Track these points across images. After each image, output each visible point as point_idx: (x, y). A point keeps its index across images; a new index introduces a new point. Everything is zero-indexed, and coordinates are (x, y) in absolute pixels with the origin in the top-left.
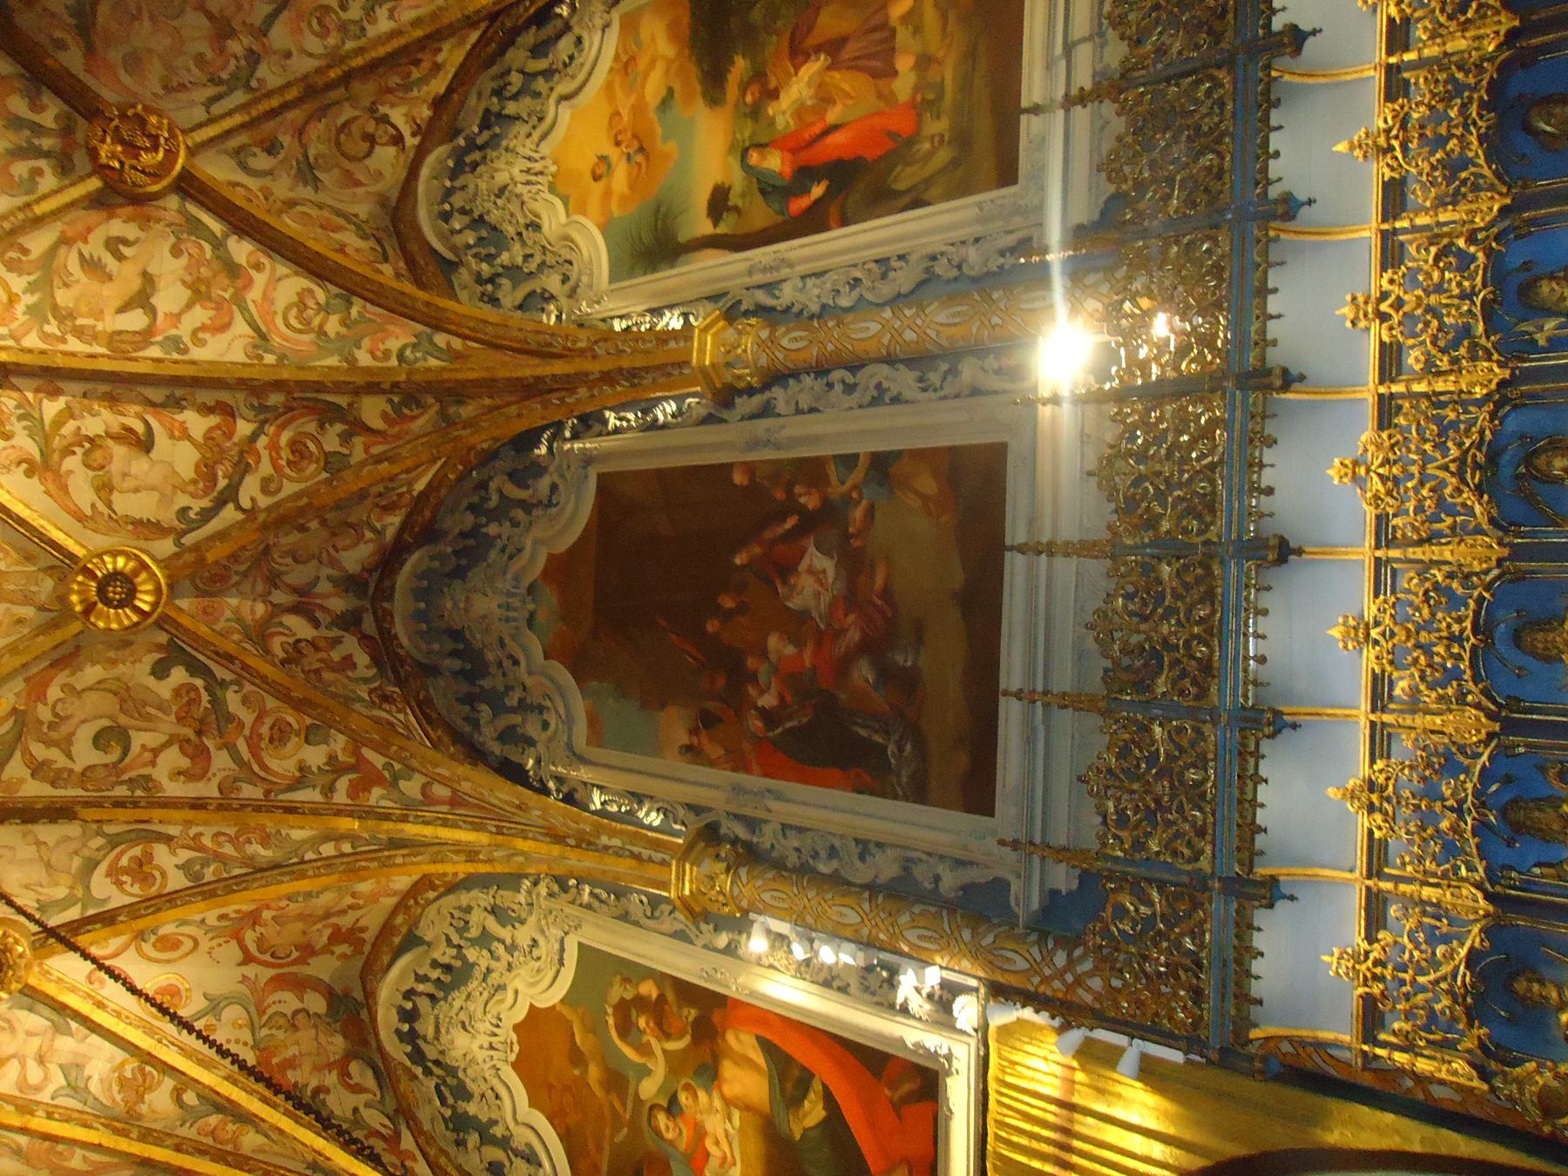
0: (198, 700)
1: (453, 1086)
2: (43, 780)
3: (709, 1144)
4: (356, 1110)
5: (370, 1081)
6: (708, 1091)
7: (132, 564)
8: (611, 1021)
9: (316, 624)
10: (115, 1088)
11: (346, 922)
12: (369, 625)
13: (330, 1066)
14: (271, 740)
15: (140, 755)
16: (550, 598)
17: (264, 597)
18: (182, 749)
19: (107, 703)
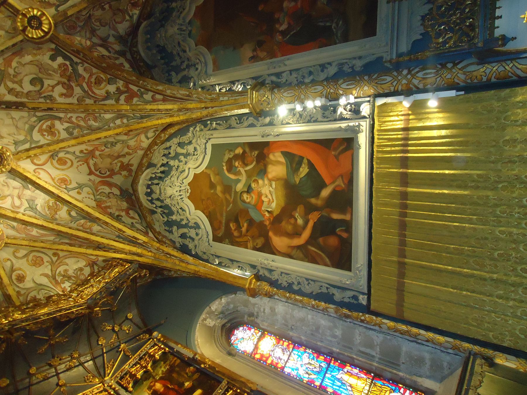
0: (67, 69)
1: (167, 211)
2: (12, 95)
3: (264, 198)
4: (132, 223)
5: (136, 216)
6: (263, 180)
7: (39, 13)
8: (225, 168)
9: (110, 52)
10: (47, 209)
11: (125, 160)
12: (129, 56)
13: (122, 210)
14: (95, 83)
15: (47, 88)
16: (197, 23)
17: (90, 39)
18: (63, 86)
19: (34, 69)
